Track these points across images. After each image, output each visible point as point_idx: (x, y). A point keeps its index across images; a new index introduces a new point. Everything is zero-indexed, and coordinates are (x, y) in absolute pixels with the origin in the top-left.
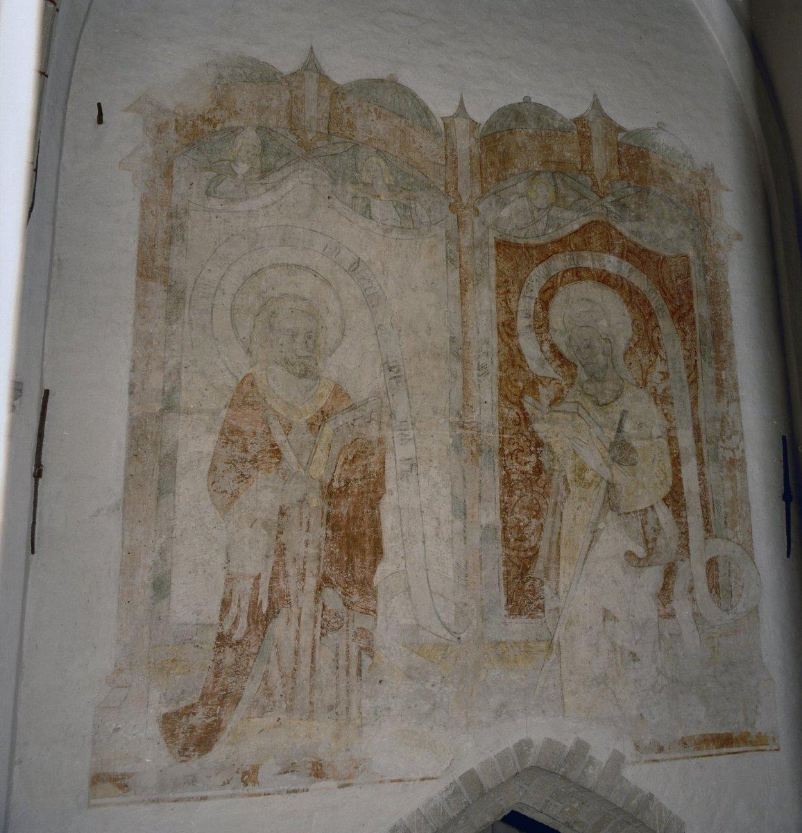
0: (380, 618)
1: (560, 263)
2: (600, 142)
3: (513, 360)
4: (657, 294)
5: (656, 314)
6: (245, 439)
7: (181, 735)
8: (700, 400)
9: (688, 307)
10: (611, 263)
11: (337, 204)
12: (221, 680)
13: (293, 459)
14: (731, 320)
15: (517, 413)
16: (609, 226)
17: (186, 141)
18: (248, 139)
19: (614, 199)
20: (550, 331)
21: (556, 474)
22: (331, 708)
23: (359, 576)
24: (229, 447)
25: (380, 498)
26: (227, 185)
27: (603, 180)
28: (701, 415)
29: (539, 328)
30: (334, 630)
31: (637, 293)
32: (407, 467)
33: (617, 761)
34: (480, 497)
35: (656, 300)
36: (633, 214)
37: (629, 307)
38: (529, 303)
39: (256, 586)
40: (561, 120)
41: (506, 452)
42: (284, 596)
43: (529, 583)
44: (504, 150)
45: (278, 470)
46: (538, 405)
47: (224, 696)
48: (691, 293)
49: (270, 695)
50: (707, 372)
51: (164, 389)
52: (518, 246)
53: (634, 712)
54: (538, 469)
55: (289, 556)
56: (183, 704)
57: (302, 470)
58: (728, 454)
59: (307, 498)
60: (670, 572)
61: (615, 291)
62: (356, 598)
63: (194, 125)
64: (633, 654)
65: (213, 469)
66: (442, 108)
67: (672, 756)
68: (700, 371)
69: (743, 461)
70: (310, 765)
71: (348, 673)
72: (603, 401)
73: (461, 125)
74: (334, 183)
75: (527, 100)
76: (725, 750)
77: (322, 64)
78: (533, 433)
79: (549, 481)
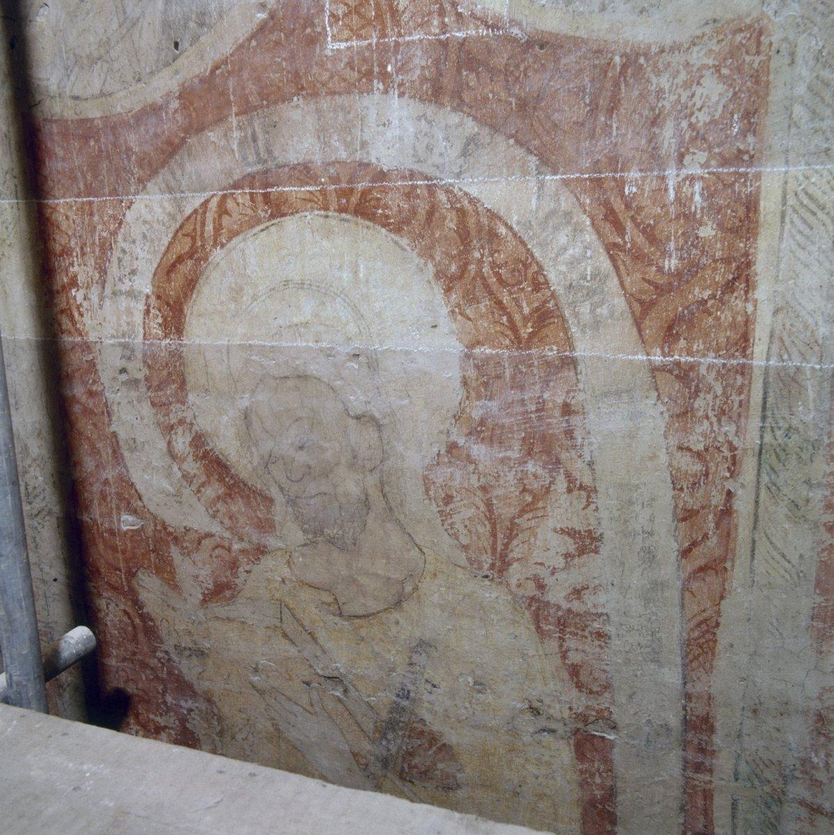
4: (578, 230)
5: (567, 313)
9: (722, 275)
15: (126, 613)
20: (191, 398)
29: (159, 388)
31: (493, 235)
38: (129, 312)
48: (751, 205)
61: (404, 242)
68: (743, 532)
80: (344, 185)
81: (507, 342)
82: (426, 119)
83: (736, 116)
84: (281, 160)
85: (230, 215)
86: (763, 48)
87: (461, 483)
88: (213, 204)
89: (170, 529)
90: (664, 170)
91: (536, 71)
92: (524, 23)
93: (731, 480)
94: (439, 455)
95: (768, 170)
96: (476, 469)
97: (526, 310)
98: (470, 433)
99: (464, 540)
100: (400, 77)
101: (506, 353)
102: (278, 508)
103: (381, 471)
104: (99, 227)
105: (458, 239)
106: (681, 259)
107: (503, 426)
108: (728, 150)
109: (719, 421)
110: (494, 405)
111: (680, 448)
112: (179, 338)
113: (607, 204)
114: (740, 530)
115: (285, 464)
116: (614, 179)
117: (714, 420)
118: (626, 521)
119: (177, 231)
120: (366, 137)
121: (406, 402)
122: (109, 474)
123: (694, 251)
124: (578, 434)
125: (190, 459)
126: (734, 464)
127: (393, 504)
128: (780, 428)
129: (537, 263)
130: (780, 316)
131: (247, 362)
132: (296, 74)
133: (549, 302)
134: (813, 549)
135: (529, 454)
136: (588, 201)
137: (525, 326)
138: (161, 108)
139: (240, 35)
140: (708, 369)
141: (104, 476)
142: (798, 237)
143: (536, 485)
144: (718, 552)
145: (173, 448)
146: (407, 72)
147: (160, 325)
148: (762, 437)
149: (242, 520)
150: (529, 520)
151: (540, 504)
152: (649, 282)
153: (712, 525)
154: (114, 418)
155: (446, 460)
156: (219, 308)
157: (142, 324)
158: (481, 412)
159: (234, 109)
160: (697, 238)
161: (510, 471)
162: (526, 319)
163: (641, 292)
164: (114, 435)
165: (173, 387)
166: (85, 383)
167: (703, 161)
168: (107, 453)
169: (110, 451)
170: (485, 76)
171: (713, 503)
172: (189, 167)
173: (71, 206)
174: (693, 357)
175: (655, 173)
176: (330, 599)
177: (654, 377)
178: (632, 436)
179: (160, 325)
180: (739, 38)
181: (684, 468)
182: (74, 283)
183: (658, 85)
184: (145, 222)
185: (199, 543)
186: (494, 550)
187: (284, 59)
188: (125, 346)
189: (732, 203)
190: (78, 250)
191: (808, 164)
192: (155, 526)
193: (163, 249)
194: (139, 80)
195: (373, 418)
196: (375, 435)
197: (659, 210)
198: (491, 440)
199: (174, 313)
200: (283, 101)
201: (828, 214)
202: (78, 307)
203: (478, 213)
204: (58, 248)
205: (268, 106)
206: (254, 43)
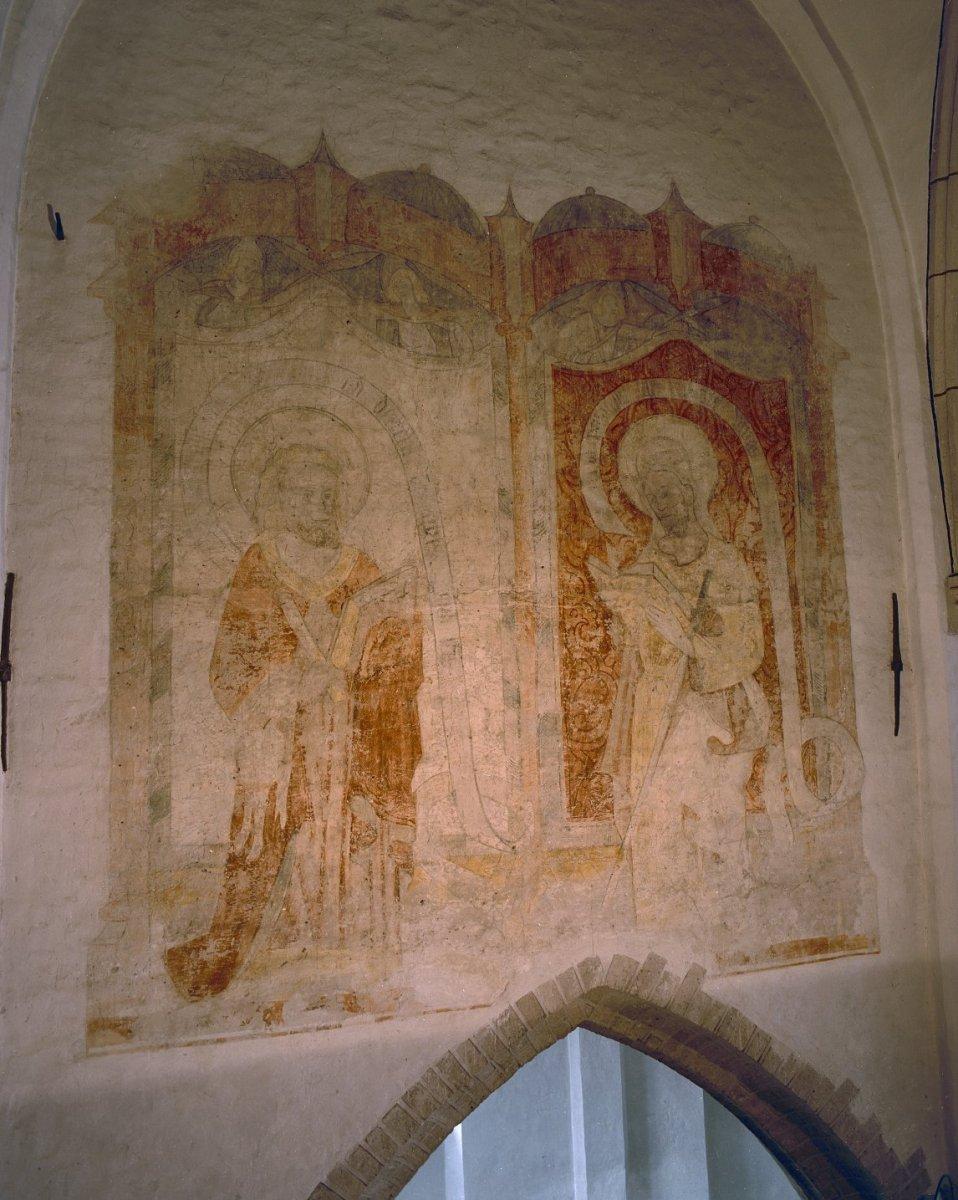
0: (419, 828)
1: (630, 394)
3: (575, 514)
6: (253, 624)
7: (191, 973)
8: (798, 556)
10: (694, 392)
11: (360, 331)
12: (234, 908)
13: (312, 645)
14: (835, 457)
16: (690, 346)
17: (168, 258)
18: (245, 255)
21: (627, 649)
22: (365, 934)
23: (394, 781)
24: (233, 632)
25: (417, 688)
26: (223, 309)
28: (798, 572)
30: (364, 845)
32: (450, 650)
33: (696, 974)
34: (537, 681)
35: (747, 435)
39: (272, 798)
40: (633, 217)
41: (568, 627)
42: (306, 810)
43: (595, 780)
44: (563, 256)
45: (293, 658)
46: (604, 567)
47: (239, 927)
49: (293, 923)
50: (807, 521)
51: (152, 567)
52: (581, 375)
53: (717, 921)
54: (606, 646)
55: (310, 759)
56: (191, 937)
57: (322, 658)
58: (830, 618)
59: (329, 691)
60: (760, 759)
62: (390, 806)
63: (179, 238)
64: (717, 856)
65: (216, 661)
66: (486, 204)
67: (759, 967)
68: (798, 519)
69: (846, 625)
70: (342, 999)
71: (383, 892)
72: (683, 560)
73: (510, 224)
74: (354, 302)
75: (590, 191)
76: (818, 956)
77: (337, 155)
78: (600, 601)
79: (618, 660)
176: (674, 558)
202: (571, 441)
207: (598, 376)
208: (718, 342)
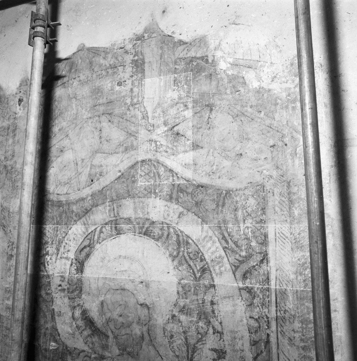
2: (154, 66)
5: (211, 269)
9: (259, 258)
19: (166, 129)
27: (154, 111)
29: (72, 292)
31: (188, 243)
36: (188, 143)
37: (176, 263)
38: (65, 264)
48: (266, 236)
68: (274, 350)
80: (141, 225)
81: (192, 279)
82: (167, 206)
83: (259, 209)
84: (121, 216)
85: (103, 233)
86: (265, 191)
87: (176, 330)
88: (98, 229)
89: (69, 349)
90: (239, 225)
91: (200, 194)
92: (197, 180)
93: (268, 330)
94: (169, 319)
95: (270, 225)
96: (182, 325)
97: (198, 268)
98: (180, 311)
99: (177, 353)
100: (160, 194)
101: (192, 282)
102: (110, 340)
103: (149, 325)
104: (59, 235)
105: (177, 245)
106: (246, 252)
107: (191, 309)
108: (258, 219)
109: (262, 307)
110: (188, 301)
111: (250, 317)
112: (81, 274)
113: (223, 234)
114: (273, 349)
115: (114, 322)
116: (225, 227)
117: (261, 307)
118: (234, 346)
119: (85, 238)
120: (149, 211)
121: (158, 299)
122: (49, 325)
123: (250, 250)
124: (216, 312)
125: (80, 320)
126: (268, 323)
127: (152, 338)
128: (282, 310)
129: (202, 252)
130: (278, 271)
131: (104, 283)
132: (128, 191)
133: (205, 265)
134: (299, 357)
135: (200, 319)
136: (217, 233)
137: (198, 273)
138: (85, 199)
139: (112, 179)
140: (257, 289)
141: (47, 326)
142: (281, 246)
143: (202, 331)
144: (267, 358)
145: (74, 315)
146: (162, 192)
147: (75, 269)
148: (277, 314)
149: (97, 345)
150: (200, 345)
151: (204, 339)
152: (237, 259)
153: (263, 347)
154: (54, 303)
155: (171, 321)
156: (96, 264)
157: (69, 269)
158: (184, 303)
159: (108, 200)
160: (251, 246)
161: (193, 326)
162: (198, 271)
163: (234, 263)
164: (53, 309)
165: (77, 292)
166: (45, 290)
167: (251, 222)
168: (49, 317)
169: (50, 316)
170: (185, 194)
171: (263, 338)
172: (92, 217)
173: (51, 228)
174: (252, 285)
175: (237, 225)
177: (240, 292)
178: (234, 312)
179: (75, 269)
180: (258, 187)
181: (252, 325)
182: (47, 254)
183: (236, 199)
184: (75, 234)
185: (79, 355)
186: (188, 357)
187: (125, 187)
188: (62, 277)
189: (260, 235)
190: (51, 242)
191: (281, 224)
192: (63, 347)
193: (80, 243)
194: (79, 190)
195: (146, 305)
196: (147, 311)
197: (239, 237)
198: (187, 314)
199: (81, 265)
200: (124, 199)
201: (289, 239)
202: (47, 262)
203: (183, 236)
204: (44, 241)
205: (119, 200)
206: (116, 181)
207: (73, 203)
208: (187, 154)
